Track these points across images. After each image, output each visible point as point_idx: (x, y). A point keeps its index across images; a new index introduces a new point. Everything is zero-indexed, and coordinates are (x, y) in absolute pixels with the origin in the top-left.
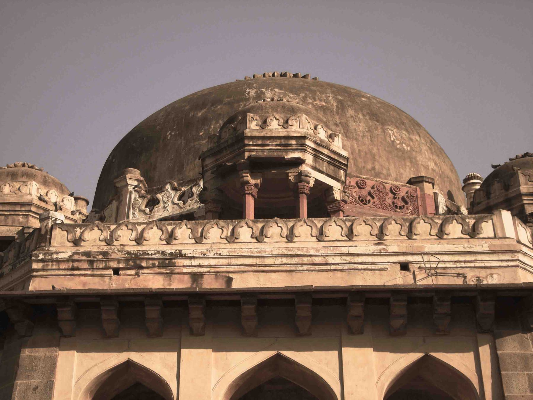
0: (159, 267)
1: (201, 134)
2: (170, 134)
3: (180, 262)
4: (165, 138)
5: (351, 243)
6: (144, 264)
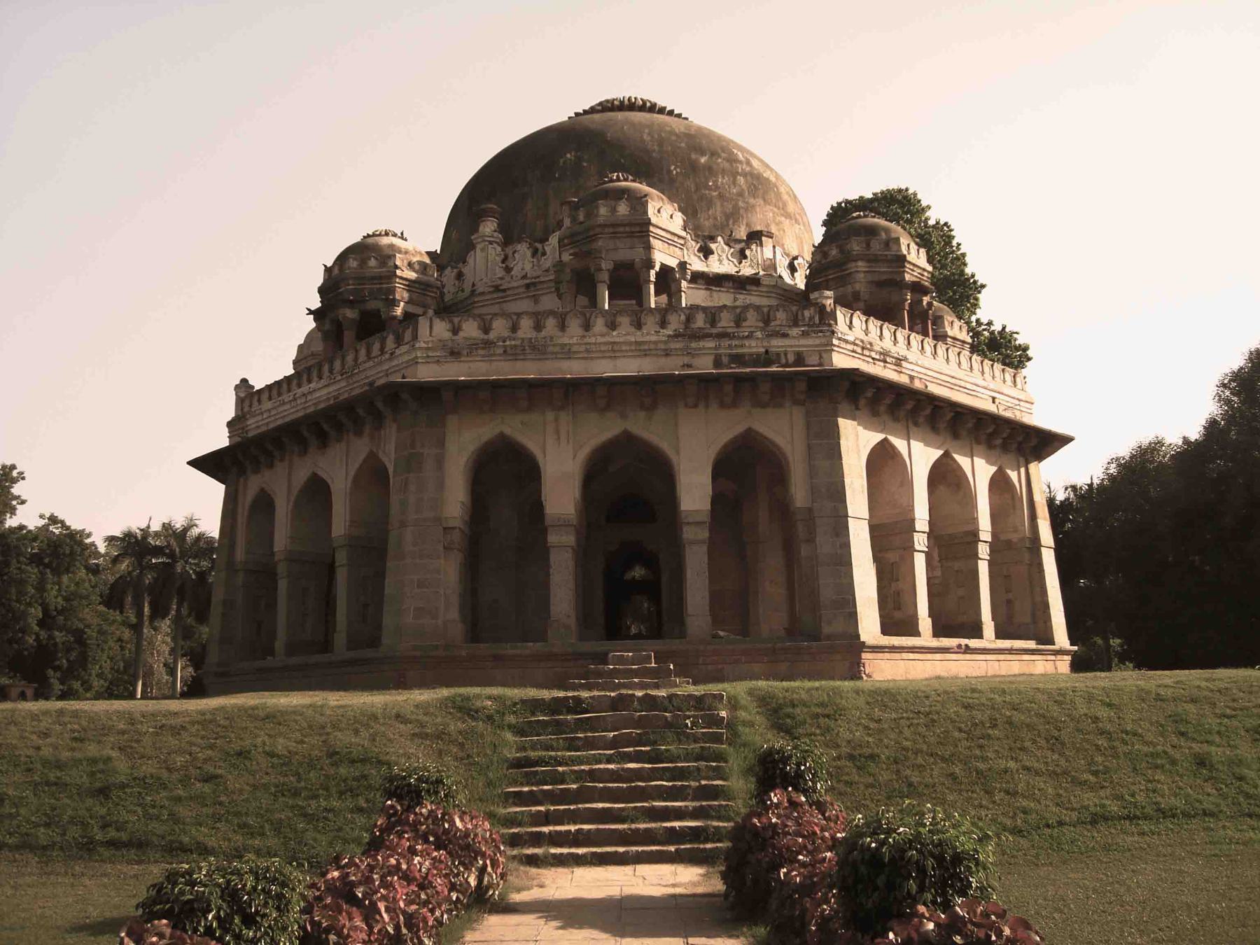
0: (895, 365)
1: (710, 184)
2: (675, 169)
3: (904, 364)
4: (670, 172)
5: (969, 373)
6: (888, 360)
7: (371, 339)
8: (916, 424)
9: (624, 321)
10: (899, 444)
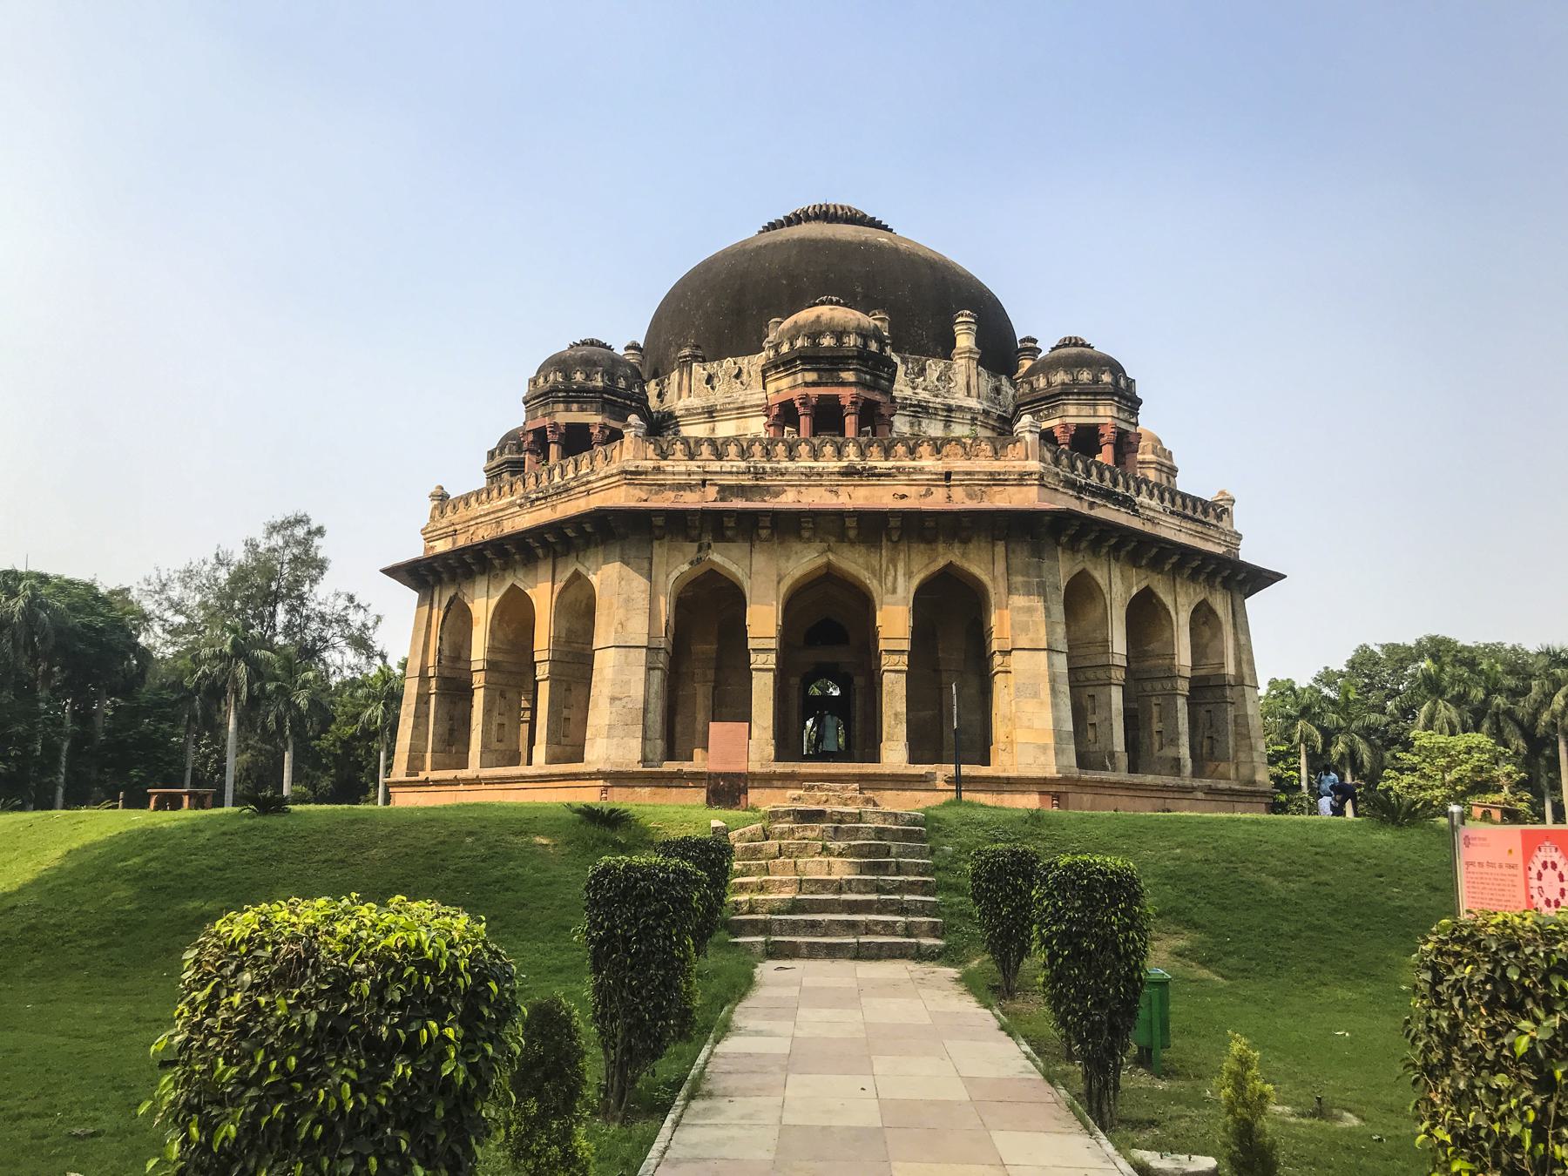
7: (580, 457)
8: (1117, 560)
9: (828, 449)
10: (1100, 576)
